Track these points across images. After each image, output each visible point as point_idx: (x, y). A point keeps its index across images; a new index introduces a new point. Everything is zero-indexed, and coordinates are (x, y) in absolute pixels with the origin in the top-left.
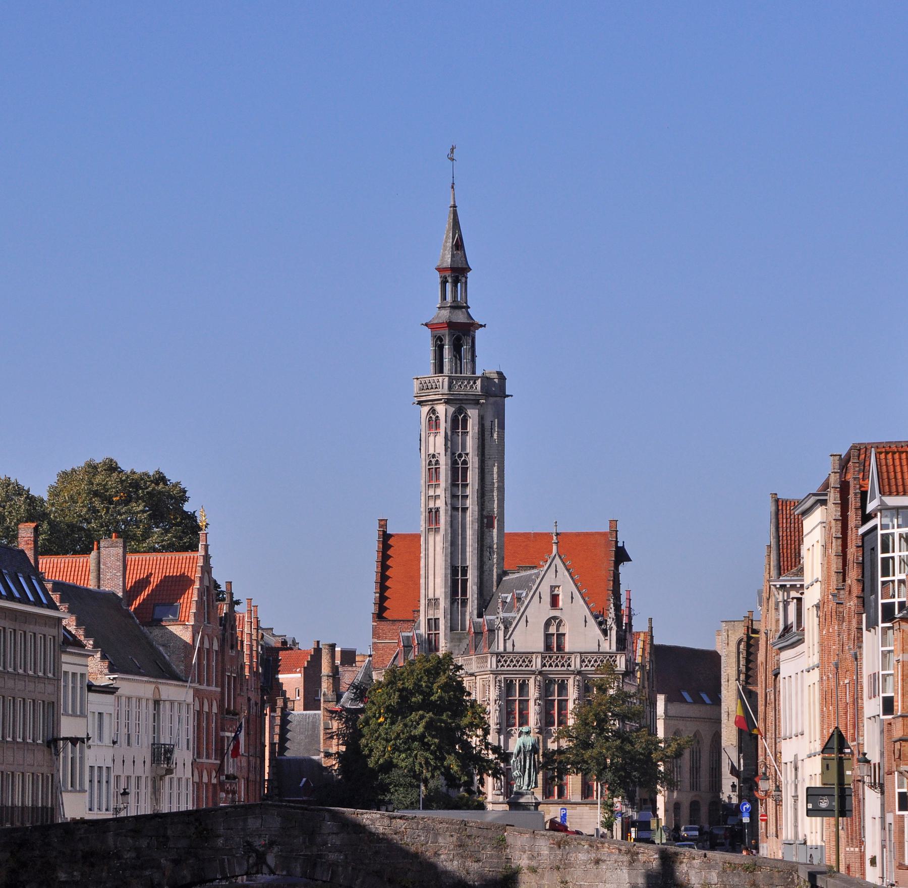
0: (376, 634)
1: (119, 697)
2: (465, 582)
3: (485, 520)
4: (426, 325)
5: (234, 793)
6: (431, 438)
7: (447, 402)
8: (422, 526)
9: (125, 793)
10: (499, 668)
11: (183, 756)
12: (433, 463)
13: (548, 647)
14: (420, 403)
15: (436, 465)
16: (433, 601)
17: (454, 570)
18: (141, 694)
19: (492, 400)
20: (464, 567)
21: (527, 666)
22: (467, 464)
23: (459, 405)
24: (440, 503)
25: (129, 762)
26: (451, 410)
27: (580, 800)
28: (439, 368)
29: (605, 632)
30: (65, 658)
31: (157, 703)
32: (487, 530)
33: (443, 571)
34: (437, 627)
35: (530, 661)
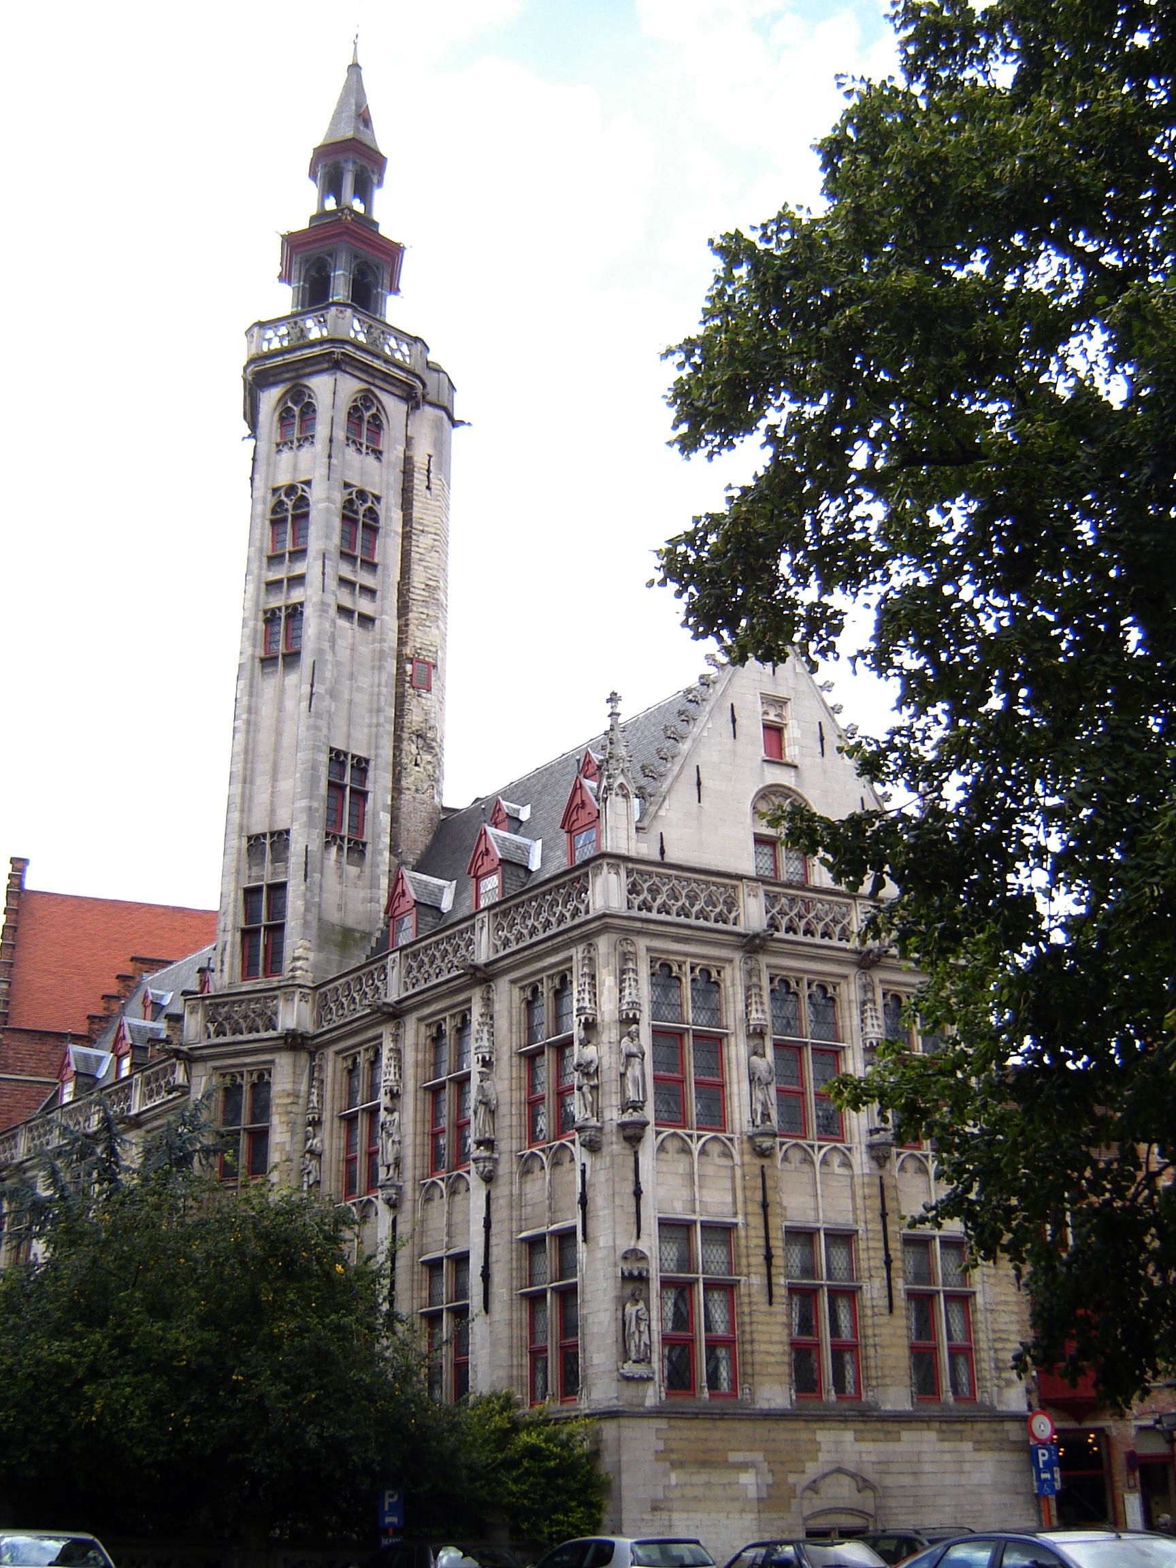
2: (360, 796)
10: (635, 913)
12: (289, 504)
15: (295, 507)
16: (268, 842)
17: (337, 758)
20: (360, 760)
21: (721, 918)
22: (376, 520)
23: (364, 386)
26: (351, 385)
27: (907, 1406)
32: (411, 691)
35: (731, 904)
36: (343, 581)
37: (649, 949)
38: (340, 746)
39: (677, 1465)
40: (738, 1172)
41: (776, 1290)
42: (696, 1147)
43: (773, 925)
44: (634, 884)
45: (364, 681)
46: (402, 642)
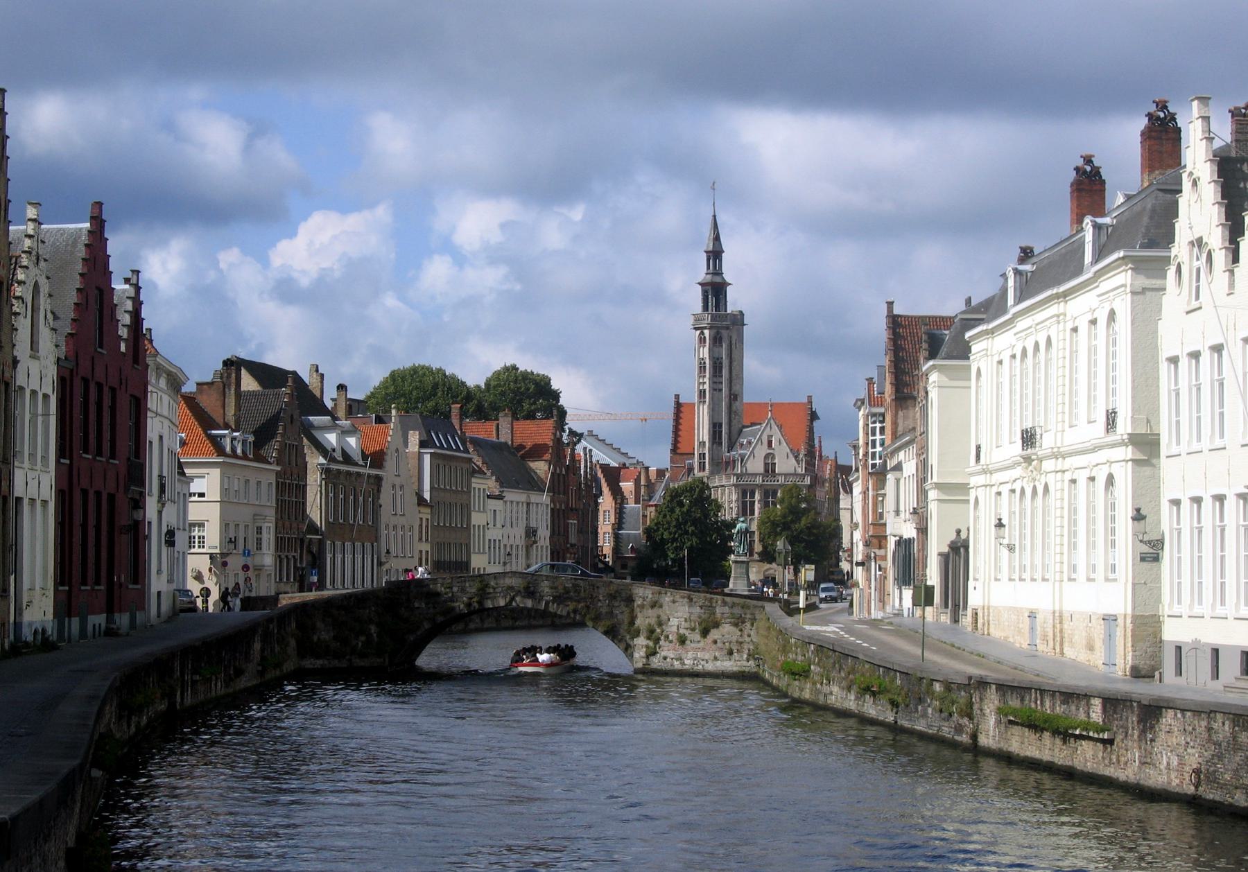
0: (672, 461)
1: (505, 502)
4: (699, 284)
5: (575, 554)
6: (701, 349)
7: (710, 328)
8: (696, 400)
9: (509, 554)
11: (544, 534)
13: (766, 470)
14: (696, 329)
18: (518, 500)
19: (736, 327)
24: (707, 387)
25: (512, 538)
26: (714, 331)
28: (705, 308)
29: (798, 462)
30: (473, 480)
31: (528, 504)
33: (708, 426)
34: (704, 458)
38: (715, 421)
43: (763, 481)
46: (730, 390)
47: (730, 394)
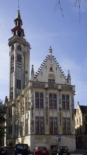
2: (20, 84)
3: (25, 72)
17: (17, 81)
26: (18, 44)
36: (18, 64)
37: (35, 90)
38: (18, 79)
39: (36, 139)
40: (44, 112)
41: (48, 123)
42: (40, 110)
44: (33, 84)
45: (20, 73)
46: (25, 70)
47: (25, 71)
